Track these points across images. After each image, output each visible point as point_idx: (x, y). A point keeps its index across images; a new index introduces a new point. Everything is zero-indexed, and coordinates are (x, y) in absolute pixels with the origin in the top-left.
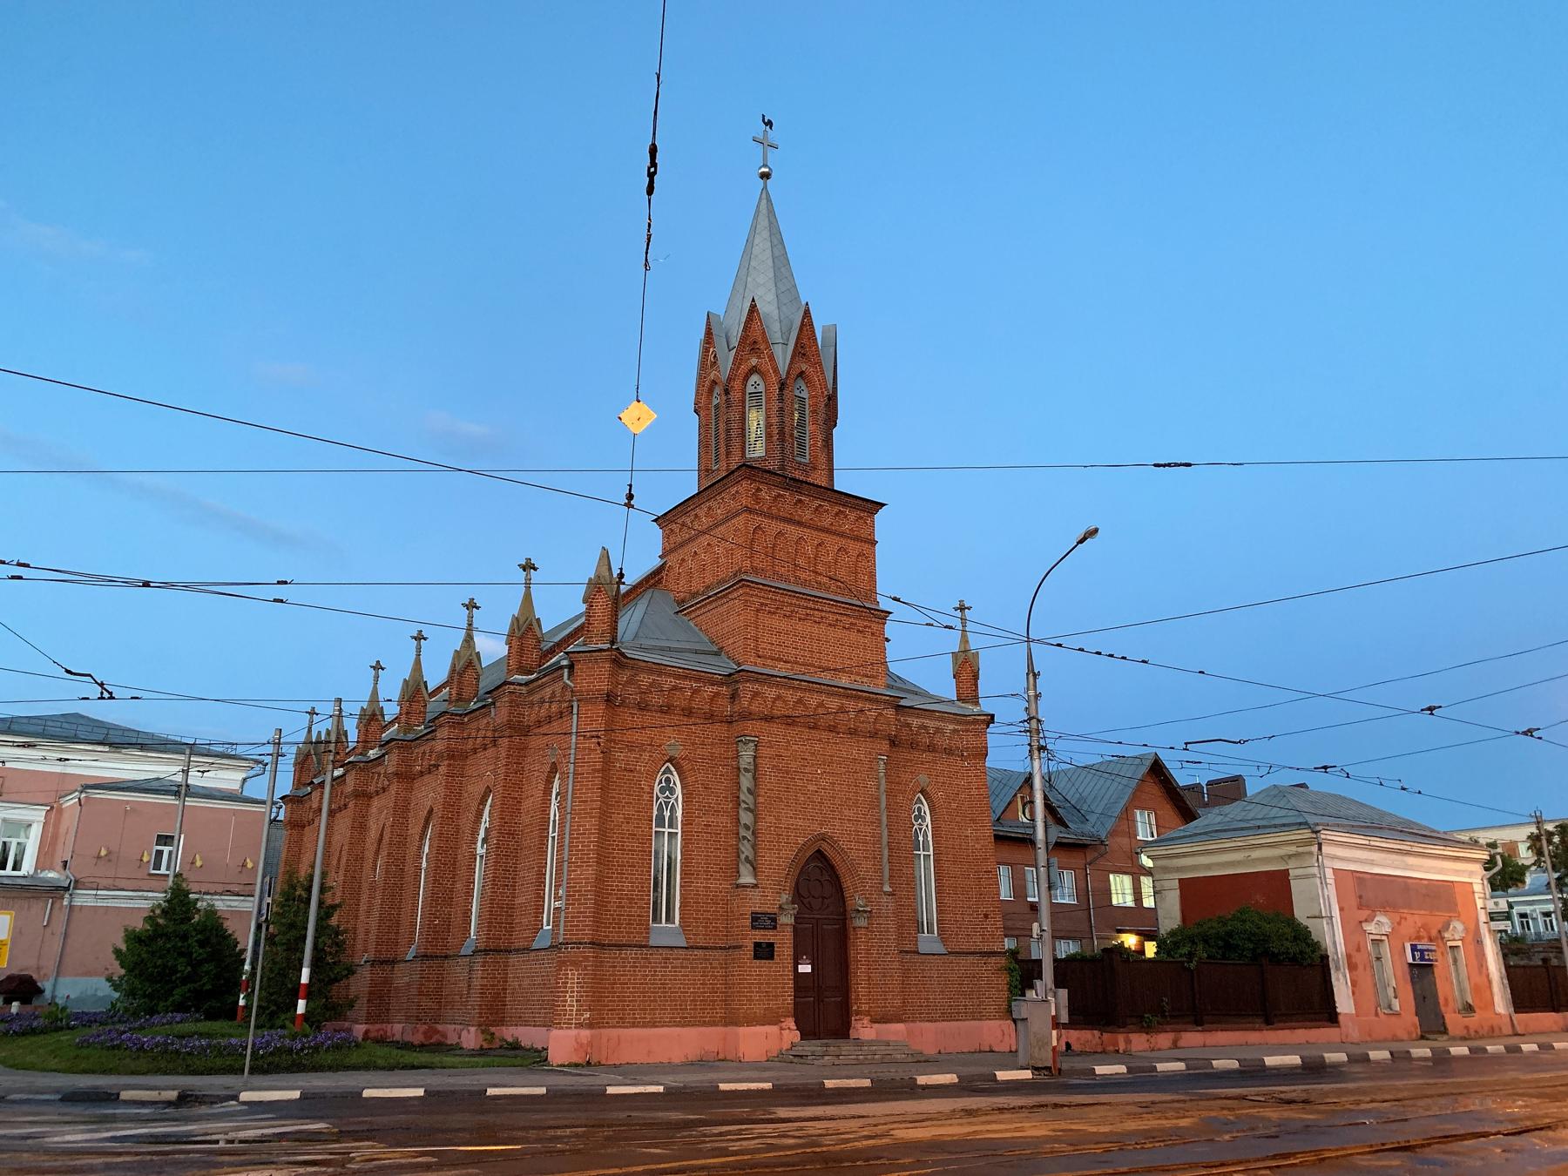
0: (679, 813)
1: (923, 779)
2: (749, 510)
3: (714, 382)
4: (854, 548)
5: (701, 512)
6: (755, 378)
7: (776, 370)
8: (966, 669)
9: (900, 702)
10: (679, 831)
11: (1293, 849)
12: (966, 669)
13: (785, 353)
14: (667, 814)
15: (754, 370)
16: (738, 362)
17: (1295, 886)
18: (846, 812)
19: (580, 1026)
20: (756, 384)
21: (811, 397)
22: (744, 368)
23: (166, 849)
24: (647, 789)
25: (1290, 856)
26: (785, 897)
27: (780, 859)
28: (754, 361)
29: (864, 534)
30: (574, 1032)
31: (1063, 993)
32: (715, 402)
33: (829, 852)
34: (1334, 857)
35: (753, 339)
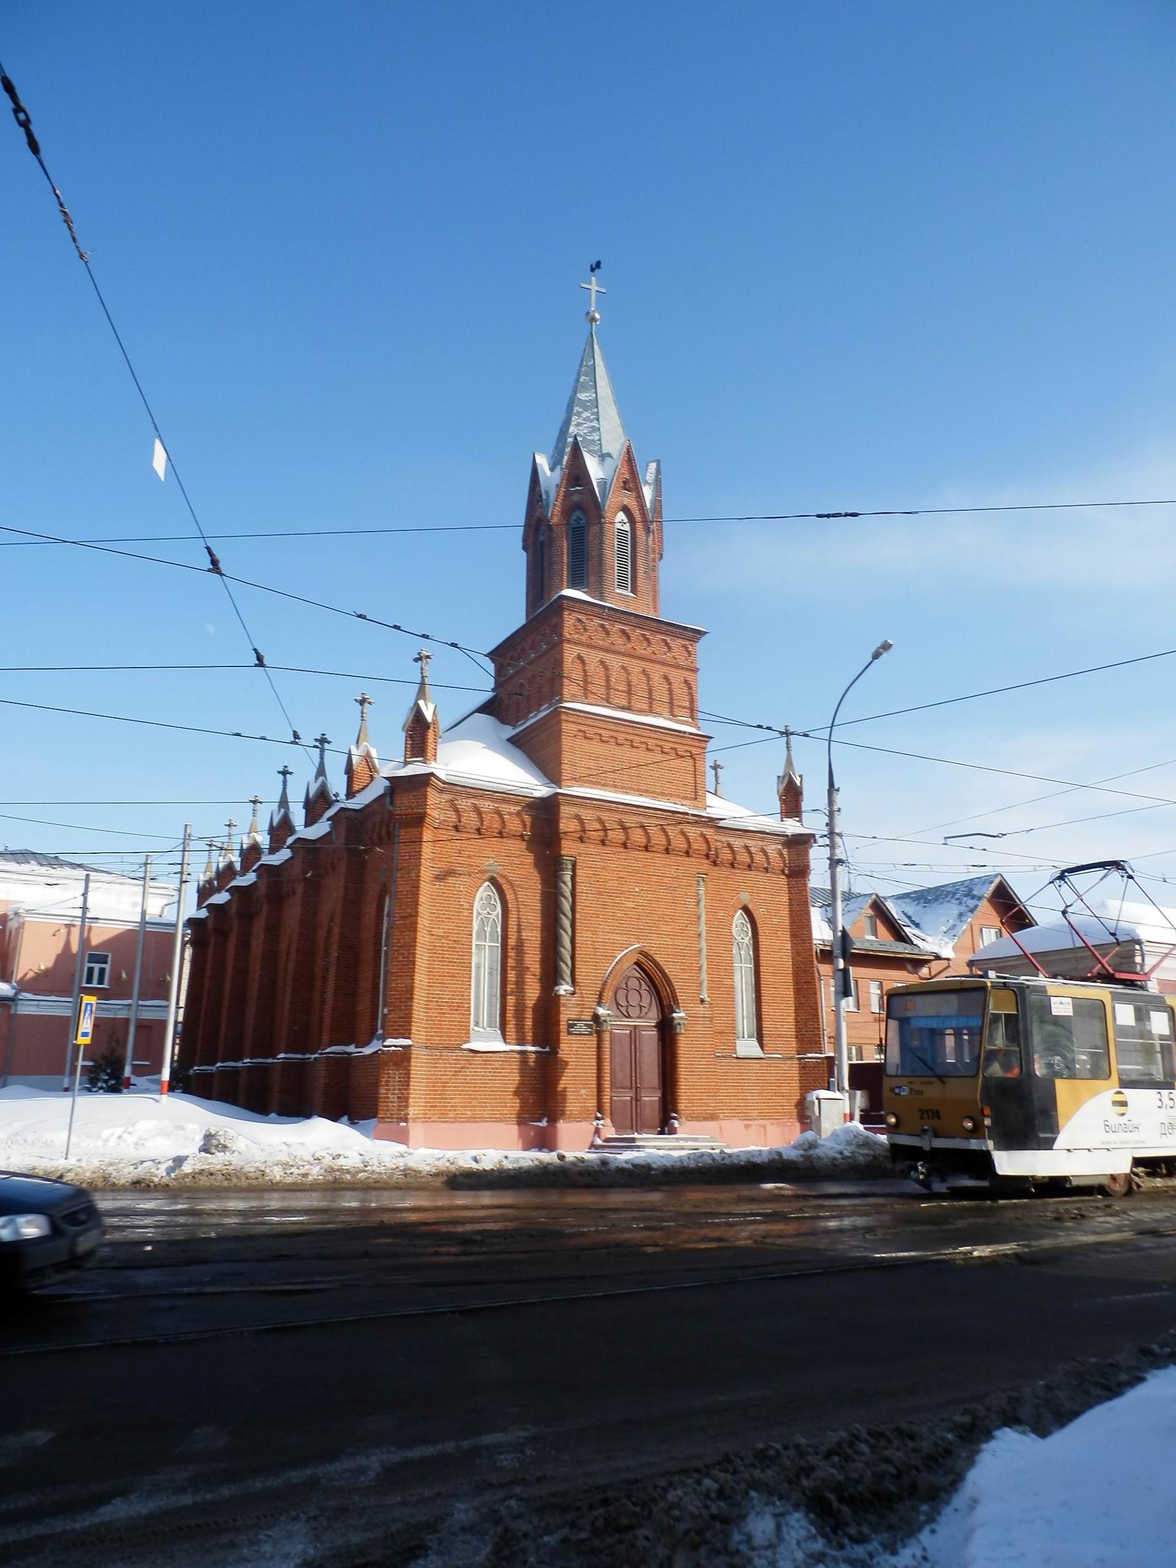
1: (745, 897)
4: (677, 676)
6: (578, 514)
14: (488, 929)
21: (633, 529)
24: (466, 906)
33: (648, 965)
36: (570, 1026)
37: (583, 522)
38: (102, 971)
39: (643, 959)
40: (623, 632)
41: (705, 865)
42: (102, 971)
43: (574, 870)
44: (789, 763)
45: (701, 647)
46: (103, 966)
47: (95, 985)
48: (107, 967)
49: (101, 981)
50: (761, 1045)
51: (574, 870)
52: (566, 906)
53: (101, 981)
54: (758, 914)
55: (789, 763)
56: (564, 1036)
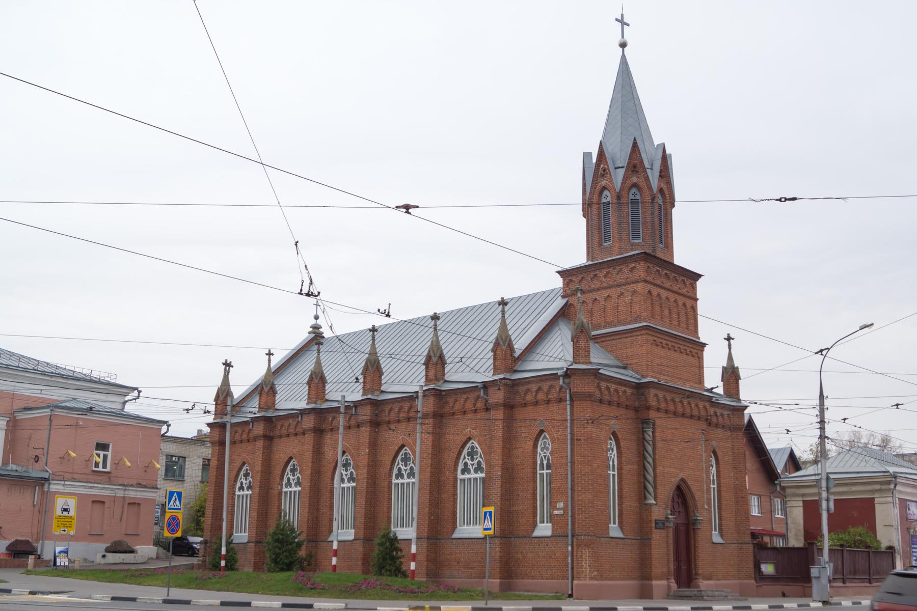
0: (616, 463)
1: (714, 443)
2: (645, 281)
3: (604, 188)
4: (689, 303)
5: (601, 274)
6: (634, 190)
7: (650, 188)
8: (731, 375)
9: (709, 400)
10: (616, 473)
11: (878, 487)
12: (731, 375)
13: (652, 174)
15: (635, 185)
16: (625, 178)
17: (878, 509)
18: (690, 464)
19: (591, 579)
20: (634, 194)
22: (629, 183)
23: (102, 453)
25: (877, 491)
26: (669, 512)
27: (666, 491)
28: (634, 179)
29: (692, 295)
30: (588, 582)
31: (832, 565)
32: (604, 200)
33: (683, 487)
34: (900, 492)
35: (635, 165)
36: (656, 523)
37: (638, 197)
38: (105, 457)
39: (682, 484)
40: (658, 271)
41: (704, 425)
42: (105, 457)
43: (654, 428)
44: (730, 358)
45: (699, 284)
46: (106, 453)
47: (100, 469)
48: (109, 454)
49: (104, 466)
50: (722, 536)
51: (654, 428)
52: (650, 449)
53: (104, 466)
54: (720, 454)
55: (730, 358)
56: (654, 530)
